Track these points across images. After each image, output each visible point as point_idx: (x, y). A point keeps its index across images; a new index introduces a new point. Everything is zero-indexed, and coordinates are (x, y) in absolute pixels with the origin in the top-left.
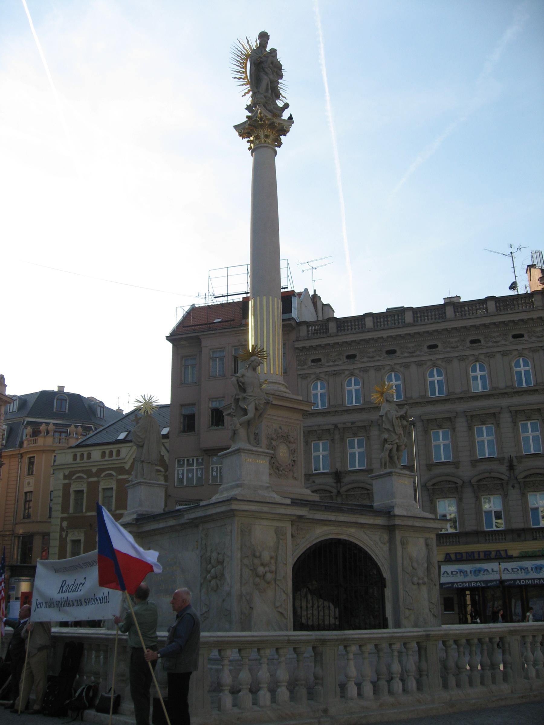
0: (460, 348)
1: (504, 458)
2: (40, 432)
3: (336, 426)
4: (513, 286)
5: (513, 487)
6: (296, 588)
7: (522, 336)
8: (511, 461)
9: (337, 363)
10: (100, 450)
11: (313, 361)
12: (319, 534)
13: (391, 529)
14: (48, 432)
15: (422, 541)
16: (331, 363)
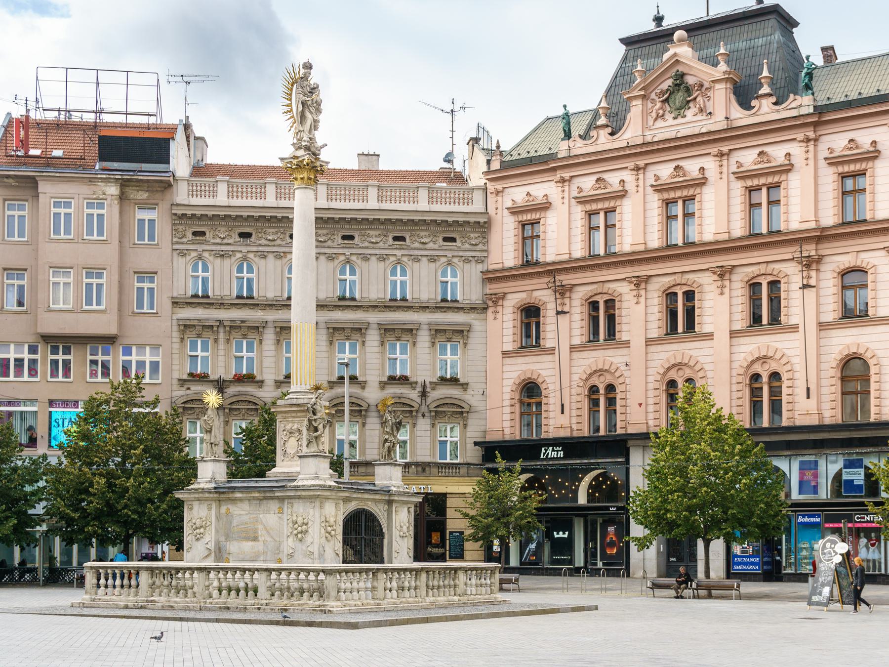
0: (381, 245)
1: (416, 383)
3: (221, 322)
4: (448, 158)
5: (423, 416)
6: (346, 542)
7: (453, 240)
8: (424, 387)
9: (225, 241)
11: (195, 234)
12: (353, 506)
13: (390, 503)
15: (406, 509)
16: (218, 241)
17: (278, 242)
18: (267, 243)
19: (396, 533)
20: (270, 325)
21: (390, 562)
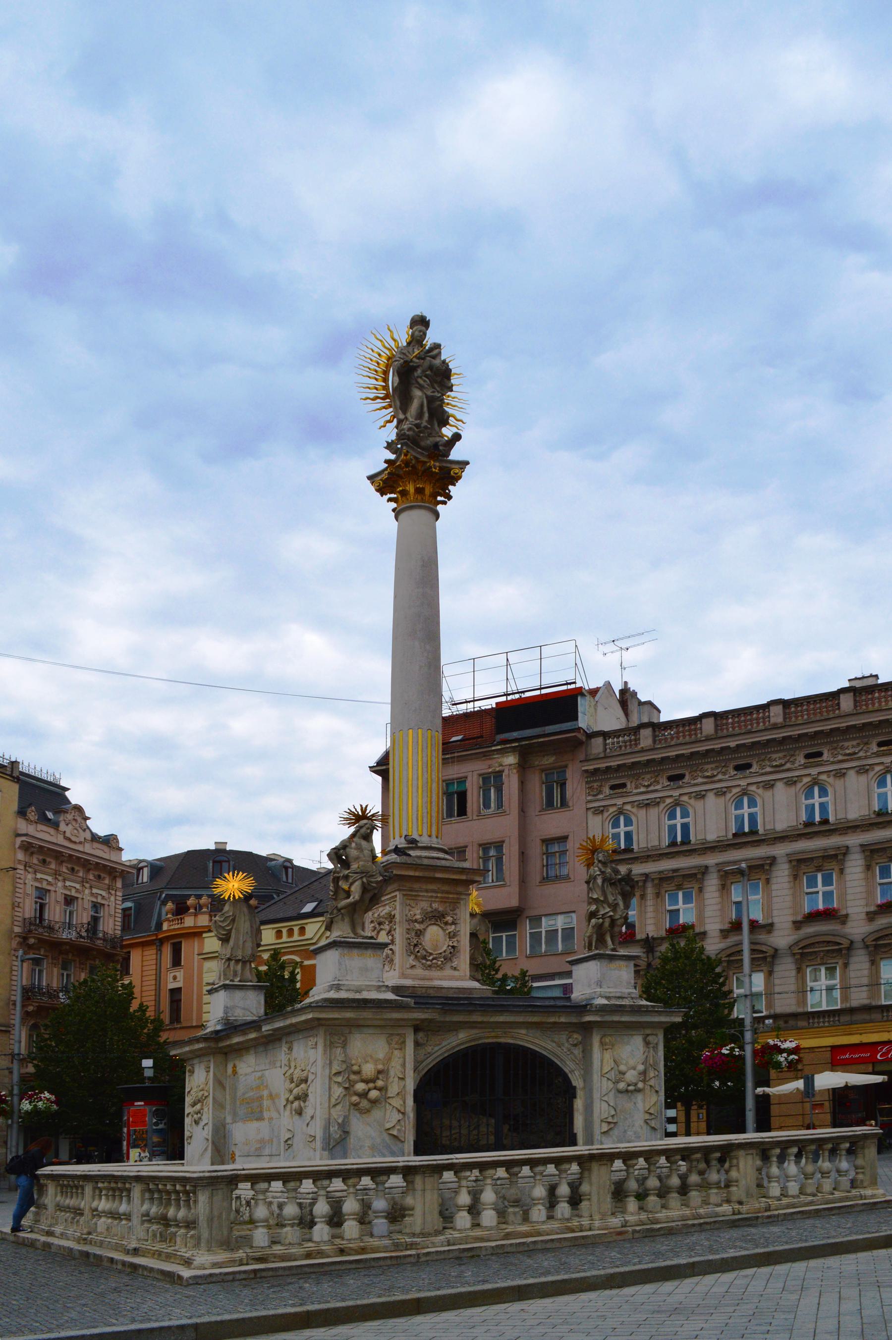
11: (613, 787)
18: (705, 780)
21: (589, 1141)
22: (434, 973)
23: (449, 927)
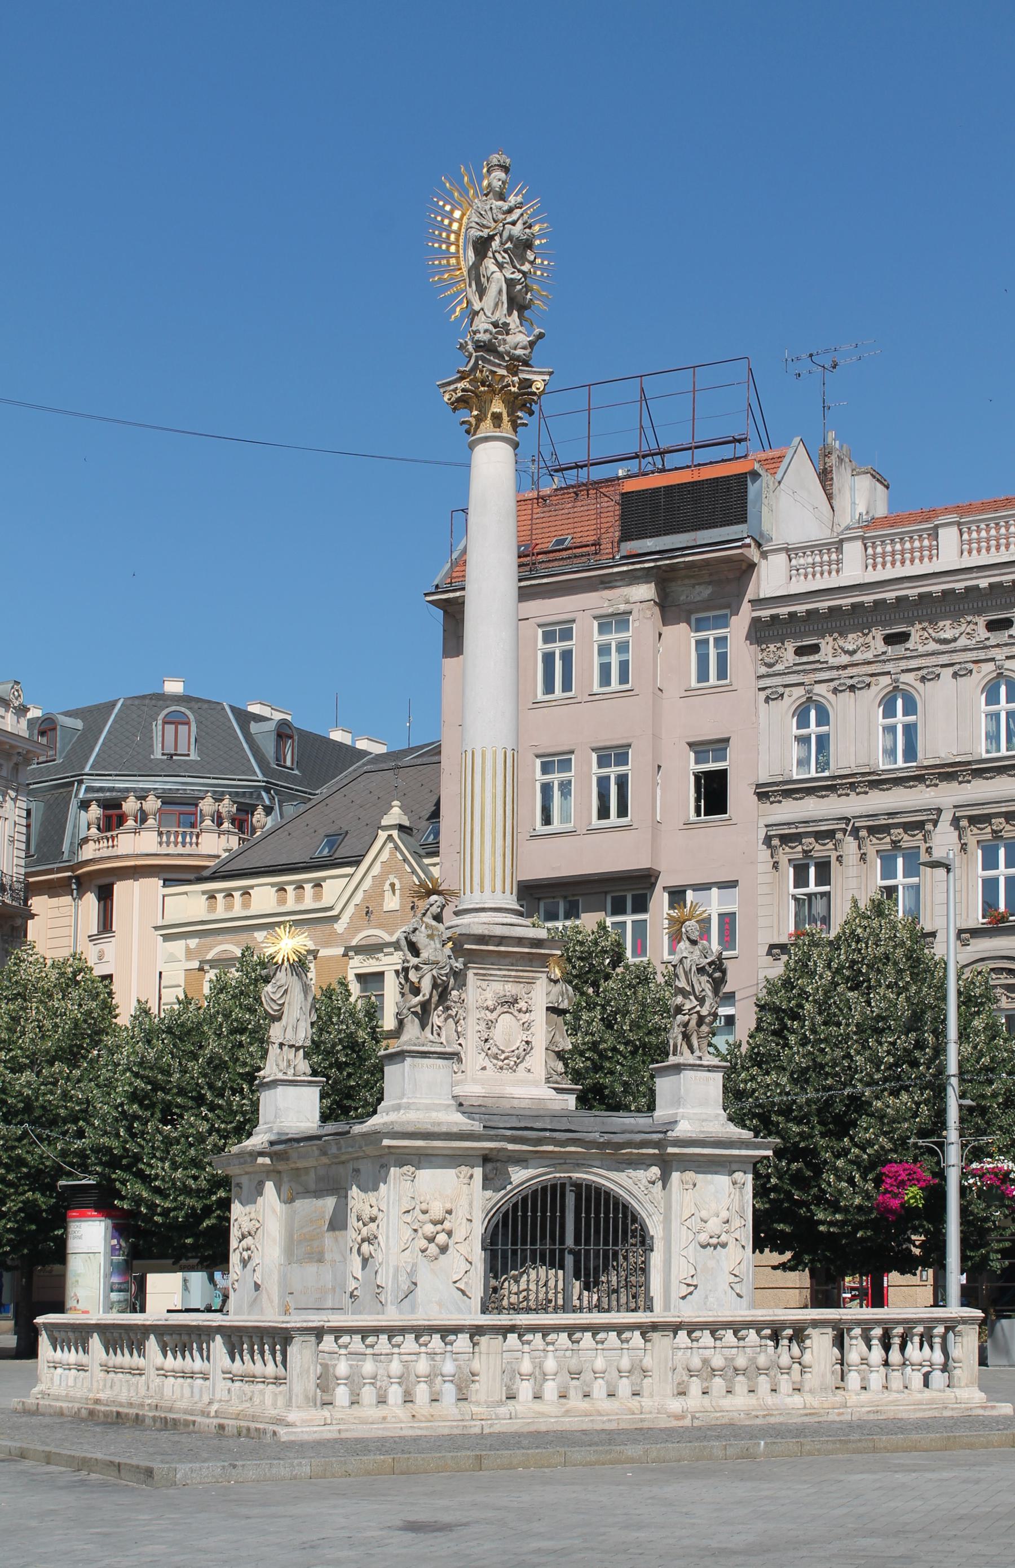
2: (122, 819)
10: (273, 885)
14: (142, 817)
17: (963, 642)
19: (681, 1236)
20: (946, 817)
22: (506, 1074)
23: (522, 1015)
